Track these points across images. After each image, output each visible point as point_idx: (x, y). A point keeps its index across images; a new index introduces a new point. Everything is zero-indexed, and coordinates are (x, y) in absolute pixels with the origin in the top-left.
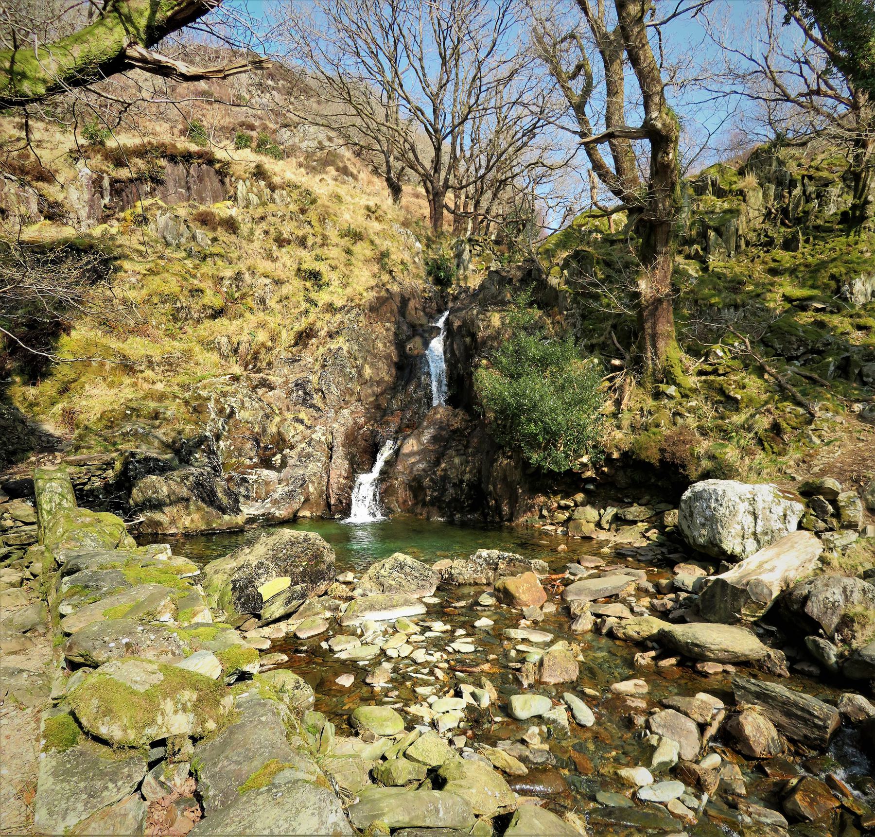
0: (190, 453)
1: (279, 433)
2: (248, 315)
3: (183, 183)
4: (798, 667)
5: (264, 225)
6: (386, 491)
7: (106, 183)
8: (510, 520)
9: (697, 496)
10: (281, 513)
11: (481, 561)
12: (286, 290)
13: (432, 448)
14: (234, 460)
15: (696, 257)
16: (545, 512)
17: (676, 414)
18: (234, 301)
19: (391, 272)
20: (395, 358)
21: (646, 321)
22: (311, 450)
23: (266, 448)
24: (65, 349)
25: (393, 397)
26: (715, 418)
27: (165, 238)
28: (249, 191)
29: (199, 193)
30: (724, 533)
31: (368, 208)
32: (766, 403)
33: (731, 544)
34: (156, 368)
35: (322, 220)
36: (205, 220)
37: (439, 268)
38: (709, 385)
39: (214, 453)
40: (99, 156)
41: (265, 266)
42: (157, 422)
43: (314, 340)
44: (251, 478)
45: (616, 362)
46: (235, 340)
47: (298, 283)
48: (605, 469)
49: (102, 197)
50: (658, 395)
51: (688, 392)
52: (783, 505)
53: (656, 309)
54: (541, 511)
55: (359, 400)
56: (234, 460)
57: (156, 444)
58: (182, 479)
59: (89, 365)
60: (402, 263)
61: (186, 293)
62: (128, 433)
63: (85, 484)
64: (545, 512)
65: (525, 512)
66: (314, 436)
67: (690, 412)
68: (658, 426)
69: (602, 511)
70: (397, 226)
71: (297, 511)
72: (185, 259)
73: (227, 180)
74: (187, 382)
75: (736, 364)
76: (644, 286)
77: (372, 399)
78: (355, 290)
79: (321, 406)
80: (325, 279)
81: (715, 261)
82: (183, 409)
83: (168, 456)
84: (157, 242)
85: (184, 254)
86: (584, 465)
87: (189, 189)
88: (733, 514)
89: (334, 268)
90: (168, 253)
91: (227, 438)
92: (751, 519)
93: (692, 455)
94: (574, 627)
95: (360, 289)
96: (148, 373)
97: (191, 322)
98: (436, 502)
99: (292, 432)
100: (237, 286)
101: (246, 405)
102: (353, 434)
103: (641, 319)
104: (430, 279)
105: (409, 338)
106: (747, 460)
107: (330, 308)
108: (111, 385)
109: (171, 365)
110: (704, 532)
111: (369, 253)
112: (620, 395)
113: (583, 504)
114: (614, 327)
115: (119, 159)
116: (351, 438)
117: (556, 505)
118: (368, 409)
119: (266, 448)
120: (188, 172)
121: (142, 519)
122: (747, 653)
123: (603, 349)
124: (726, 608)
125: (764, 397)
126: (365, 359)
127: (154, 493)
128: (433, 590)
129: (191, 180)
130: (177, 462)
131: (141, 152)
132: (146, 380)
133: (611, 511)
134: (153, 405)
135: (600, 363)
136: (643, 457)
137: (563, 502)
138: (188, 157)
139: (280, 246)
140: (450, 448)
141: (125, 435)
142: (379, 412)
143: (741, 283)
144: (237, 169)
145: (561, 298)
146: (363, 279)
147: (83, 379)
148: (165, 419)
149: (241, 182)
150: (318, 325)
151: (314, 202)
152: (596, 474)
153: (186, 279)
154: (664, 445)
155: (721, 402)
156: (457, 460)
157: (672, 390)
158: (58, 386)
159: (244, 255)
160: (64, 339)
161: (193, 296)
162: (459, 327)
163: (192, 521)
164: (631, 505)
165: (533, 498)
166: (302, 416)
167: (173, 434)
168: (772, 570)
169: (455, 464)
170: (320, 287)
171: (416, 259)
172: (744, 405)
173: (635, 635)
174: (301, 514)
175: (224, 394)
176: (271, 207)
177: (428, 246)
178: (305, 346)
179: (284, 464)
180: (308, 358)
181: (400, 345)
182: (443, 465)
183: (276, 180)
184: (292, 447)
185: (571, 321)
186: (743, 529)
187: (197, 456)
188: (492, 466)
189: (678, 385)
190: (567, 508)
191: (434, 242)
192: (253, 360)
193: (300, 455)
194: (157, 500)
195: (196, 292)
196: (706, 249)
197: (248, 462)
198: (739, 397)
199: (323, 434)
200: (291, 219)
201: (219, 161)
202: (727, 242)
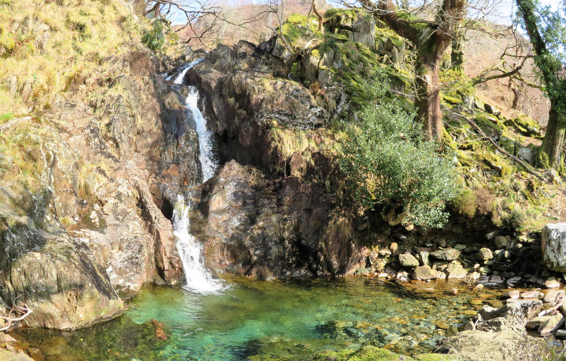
12: (58, 37)
13: (234, 204)
20: (159, 111)
22: (121, 206)
46: (22, 81)
55: (136, 151)
57: (8, 201)
66: (120, 189)
79: (117, 156)
80: (88, 31)
89: (94, 23)
99: (98, 186)
140: (263, 206)
156: (274, 218)
166: (103, 167)
169: (270, 222)
178: (75, 91)
182: (261, 224)
199: (129, 188)
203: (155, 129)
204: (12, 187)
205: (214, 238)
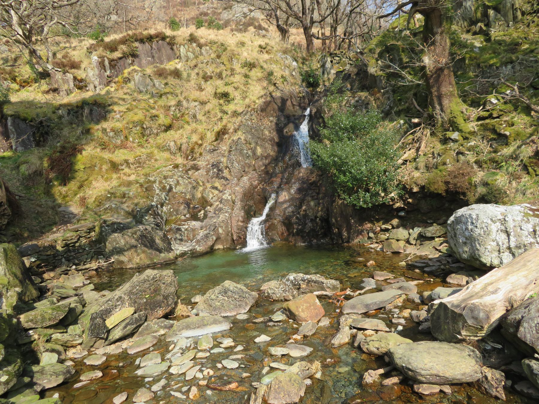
0: (142, 217)
1: (203, 197)
2: (186, 126)
3: (150, 54)
4: (518, 387)
5: (196, 71)
6: (269, 228)
7: (107, 63)
8: (348, 242)
9: (458, 221)
10: (199, 248)
11: (288, 283)
12: (208, 107)
14: (174, 217)
15: (481, 32)
16: (371, 235)
17: (459, 153)
18: (177, 119)
19: (275, 84)
20: (276, 140)
21: (433, 87)
23: (194, 208)
24: (79, 163)
25: (276, 165)
26: (490, 152)
27: (139, 88)
28: (188, 51)
29: (159, 58)
30: (482, 249)
31: (260, 46)
32: (532, 135)
33: (486, 259)
34: (131, 166)
35: (231, 60)
36: (161, 74)
37: (310, 76)
38: (485, 128)
39: (158, 214)
40: (101, 49)
41: (196, 94)
42: (124, 200)
43: (226, 136)
44: (183, 228)
45: (416, 120)
47: (215, 102)
48: (410, 200)
49: (105, 71)
50: (445, 141)
51: (467, 135)
52: (532, 223)
53: (439, 76)
54: (368, 234)
55: (255, 170)
56: (174, 217)
57: (122, 213)
58: (133, 234)
59: (94, 170)
60: (282, 77)
61: (148, 119)
62: (107, 208)
63: (76, 242)
64: (371, 235)
65: (357, 236)
66: (223, 197)
67: (469, 150)
68: (444, 164)
69: (411, 231)
70: (279, 54)
71: (213, 245)
72: (149, 99)
73: (175, 47)
74: (148, 172)
75: (509, 107)
76: (427, 60)
77: (263, 168)
78: (250, 100)
80: (232, 96)
81: (496, 33)
82: (139, 190)
83: (128, 220)
84: (135, 91)
85: (149, 96)
86: (392, 199)
87: (153, 57)
88: (488, 233)
90: (140, 97)
91: (168, 204)
92: (504, 236)
93: (470, 184)
94: (333, 342)
95: (254, 98)
96: (127, 170)
97: (152, 135)
98: (300, 233)
99: (211, 195)
100: (179, 110)
101: (181, 182)
102: (250, 192)
103: (428, 87)
104: (304, 84)
105: (286, 125)
106: (514, 184)
107: (235, 114)
108: (107, 180)
109: (140, 163)
110: (466, 249)
111: (260, 75)
112: (420, 144)
113: (398, 227)
114: (415, 95)
115: (112, 47)
116: (248, 195)
117: (379, 229)
118: (260, 175)
119: (194, 208)
120: (151, 47)
121: (113, 260)
122: (459, 377)
123: (408, 112)
124: (449, 328)
125: (529, 130)
126: (257, 143)
127: (117, 244)
128: (248, 309)
129: (154, 52)
130: (134, 223)
131: (123, 41)
132: (125, 174)
133: (417, 230)
134: (124, 189)
135: (405, 123)
136: (432, 189)
137: (383, 227)
138: (150, 38)
139: (206, 81)
141: (106, 209)
142: (268, 176)
143: (518, 44)
144: (179, 40)
145: (378, 82)
146: (257, 92)
147: (90, 179)
148: (129, 197)
149: (182, 46)
150: (229, 125)
151: (225, 50)
152: (404, 204)
153: (148, 111)
154: (448, 179)
155: (495, 139)
156: (312, 203)
157: (455, 135)
158: (78, 184)
159: (184, 90)
160: (79, 156)
161: (152, 120)
162: (315, 113)
163: (141, 259)
164: (431, 225)
165: (361, 224)
166: (217, 184)
167: (132, 206)
168: (495, 292)
170: (229, 101)
171: (294, 73)
172: (512, 139)
173: (375, 350)
174: (216, 247)
175: (165, 178)
176: (201, 58)
177: (303, 63)
178: (222, 140)
179: (205, 216)
180: (224, 147)
181: (279, 130)
183: (202, 41)
184: (211, 205)
185: (386, 96)
186: (498, 245)
187: (147, 218)
188: (332, 205)
189: (460, 131)
190: (387, 230)
191: (307, 60)
192: (191, 153)
193: (215, 210)
194: (119, 248)
195: (154, 117)
196: (488, 25)
197: (183, 217)
198: (507, 133)
199: (230, 195)
200: (212, 63)
201: (168, 37)
202: (505, 16)
203: (272, 153)
204: (127, 206)
205: (276, 219)
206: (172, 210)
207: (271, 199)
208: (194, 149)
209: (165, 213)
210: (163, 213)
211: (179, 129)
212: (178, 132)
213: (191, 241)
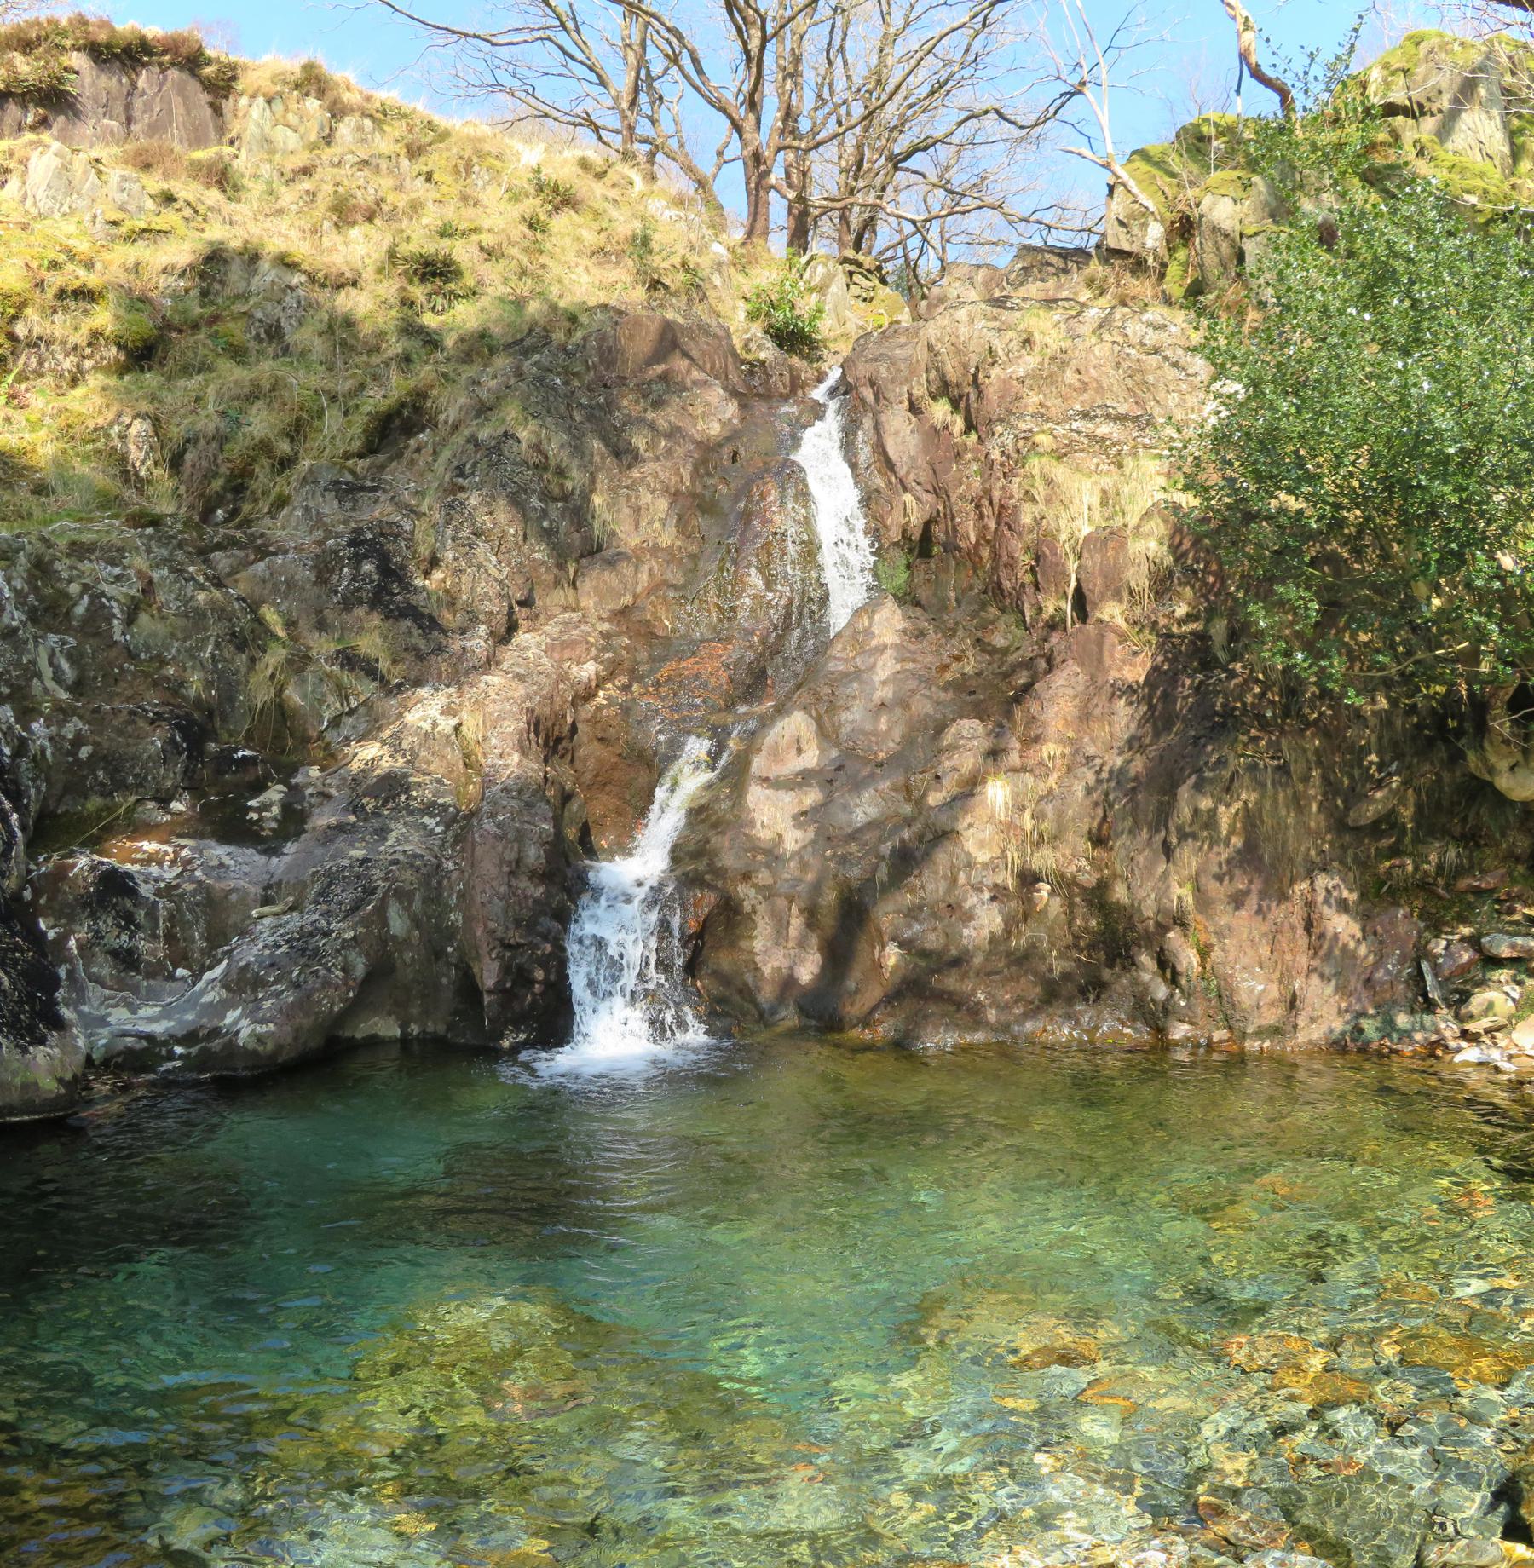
2: (225, 365)
14: (94, 803)
23: (225, 760)
46: (176, 431)
89: (489, 253)
179: (294, 819)
206: (85, 752)
207: (682, 766)
208: (251, 475)
209: (38, 761)
210: (24, 763)
211: (186, 371)
212: (182, 383)
213: (197, 977)
